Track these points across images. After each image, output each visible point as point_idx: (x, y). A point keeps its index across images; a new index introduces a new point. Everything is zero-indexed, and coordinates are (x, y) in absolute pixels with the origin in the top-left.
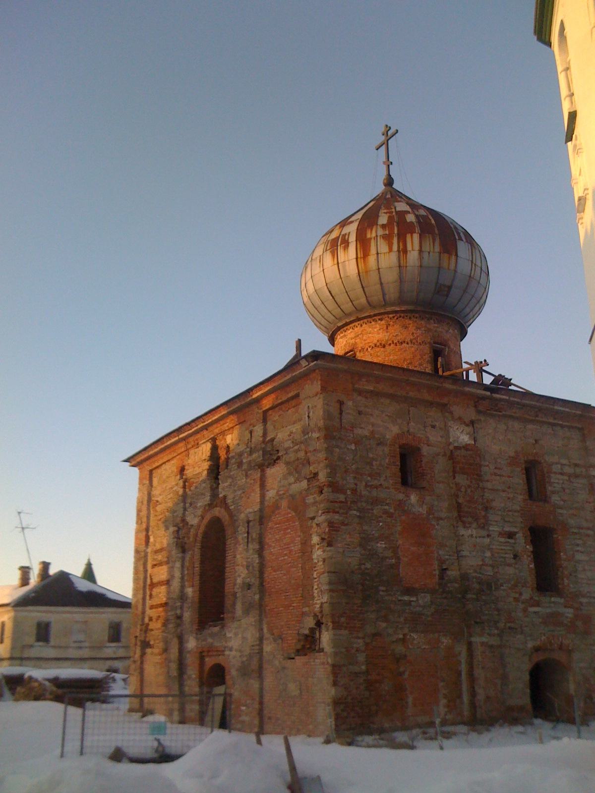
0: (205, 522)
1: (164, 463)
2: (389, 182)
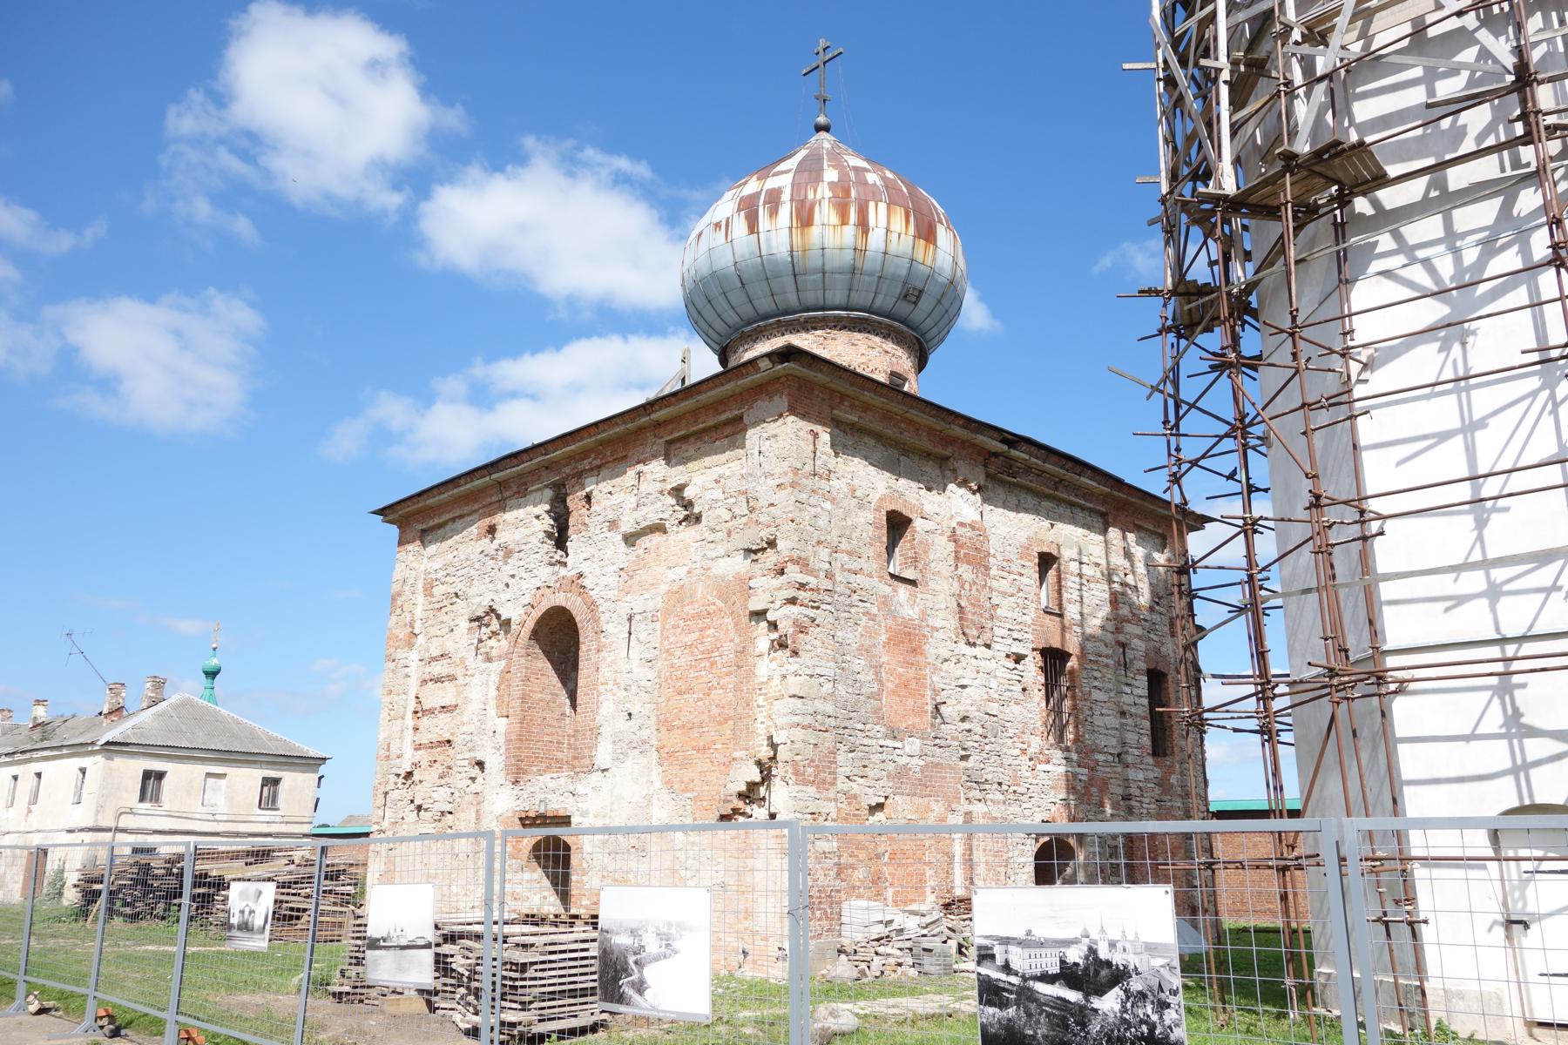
0: (537, 614)
1: (454, 520)
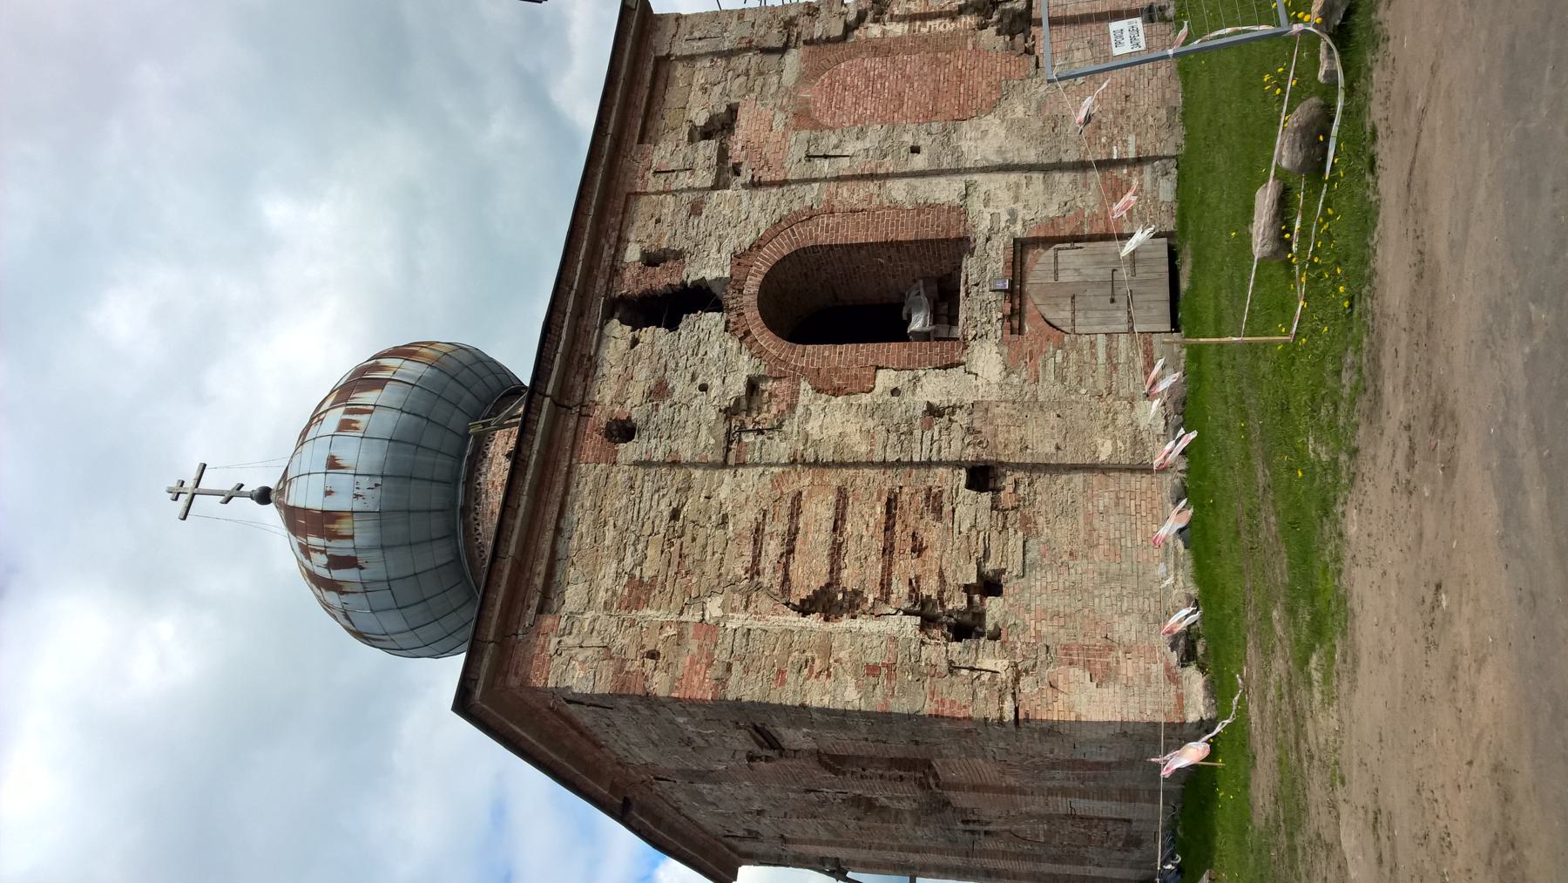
2: (264, 496)
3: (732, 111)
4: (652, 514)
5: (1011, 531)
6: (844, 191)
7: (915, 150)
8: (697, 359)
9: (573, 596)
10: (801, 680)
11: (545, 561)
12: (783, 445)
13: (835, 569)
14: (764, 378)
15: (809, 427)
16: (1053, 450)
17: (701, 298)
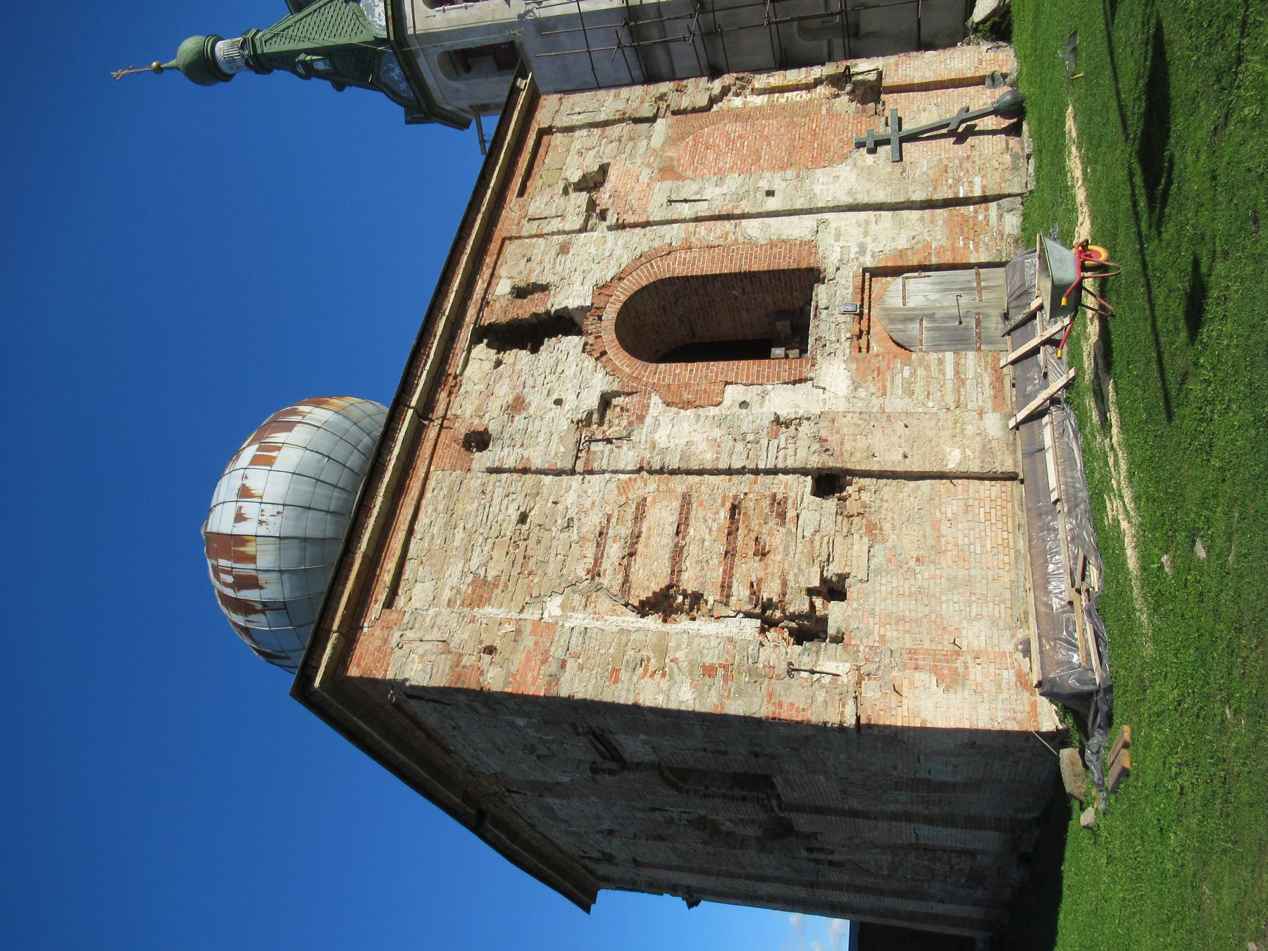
1: (410, 532)
3: (604, 170)
4: (501, 517)
5: (856, 537)
6: (702, 228)
7: (770, 193)
8: (554, 378)
9: (416, 594)
10: (635, 678)
11: (396, 559)
12: (631, 453)
13: (676, 571)
14: (616, 394)
15: (657, 436)
16: (900, 457)
17: (565, 323)
